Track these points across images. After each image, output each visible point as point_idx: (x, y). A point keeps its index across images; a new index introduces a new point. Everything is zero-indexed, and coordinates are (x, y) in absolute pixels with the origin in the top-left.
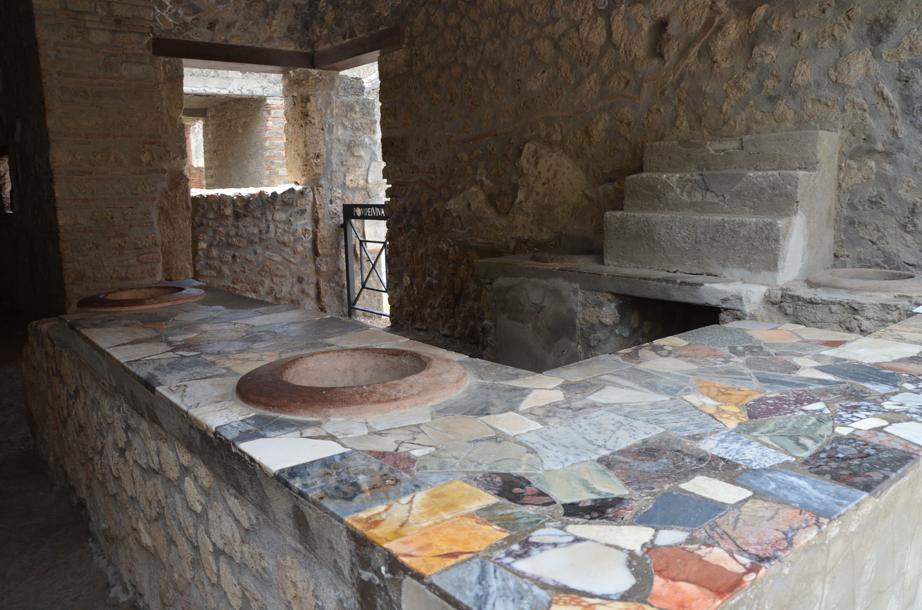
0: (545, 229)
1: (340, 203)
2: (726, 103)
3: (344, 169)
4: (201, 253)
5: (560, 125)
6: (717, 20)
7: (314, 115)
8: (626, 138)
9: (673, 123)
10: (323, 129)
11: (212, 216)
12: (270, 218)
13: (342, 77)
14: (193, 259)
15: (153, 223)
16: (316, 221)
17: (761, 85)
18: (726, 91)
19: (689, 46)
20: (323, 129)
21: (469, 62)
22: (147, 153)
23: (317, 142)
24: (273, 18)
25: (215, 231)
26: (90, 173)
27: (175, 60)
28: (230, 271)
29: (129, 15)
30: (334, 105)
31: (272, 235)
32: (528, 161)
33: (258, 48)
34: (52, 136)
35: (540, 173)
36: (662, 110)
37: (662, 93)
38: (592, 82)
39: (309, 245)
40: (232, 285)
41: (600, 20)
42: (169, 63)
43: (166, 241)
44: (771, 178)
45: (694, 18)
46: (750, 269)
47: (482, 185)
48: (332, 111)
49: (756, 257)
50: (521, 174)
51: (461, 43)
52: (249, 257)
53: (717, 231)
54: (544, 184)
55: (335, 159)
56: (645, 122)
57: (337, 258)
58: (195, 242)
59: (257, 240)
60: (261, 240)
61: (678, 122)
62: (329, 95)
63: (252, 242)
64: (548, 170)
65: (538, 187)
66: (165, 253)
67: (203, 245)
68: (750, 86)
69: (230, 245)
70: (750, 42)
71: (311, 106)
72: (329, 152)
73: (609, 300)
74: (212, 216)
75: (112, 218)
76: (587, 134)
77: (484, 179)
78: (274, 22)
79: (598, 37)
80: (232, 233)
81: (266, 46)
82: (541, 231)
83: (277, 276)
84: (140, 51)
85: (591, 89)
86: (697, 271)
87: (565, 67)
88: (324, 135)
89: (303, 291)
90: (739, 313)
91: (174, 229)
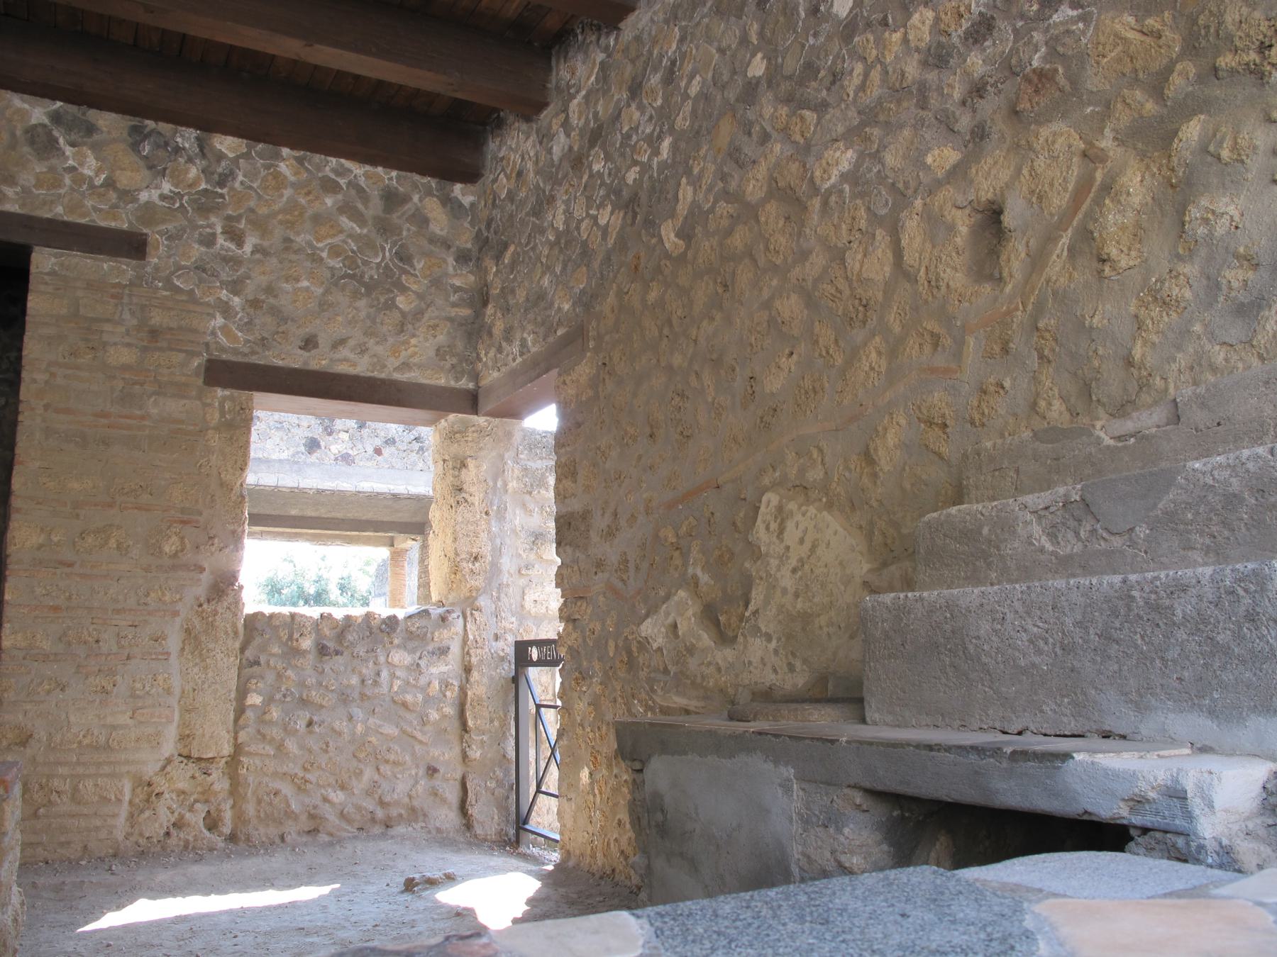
0: (798, 664)
1: (511, 639)
2: (1139, 343)
3: (522, 582)
5: (821, 450)
6: (1099, 175)
7: (472, 489)
8: (940, 456)
9: (1034, 406)
10: (487, 513)
12: (382, 659)
13: (523, 430)
14: (236, 720)
15: (168, 654)
16: (468, 670)
17: (1214, 285)
18: (1136, 316)
19: (1050, 239)
20: (487, 513)
21: (677, 360)
22: (174, 538)
23: (476, 535)
24: (414, 336)
25: (279, 676)
26: (71, 565)
28: (302, 747)
29: (174, 325)
30: (508, 474)
31: (385, 689)
32: (767, 528)
33: (383, 381)
35: (788, 548)
36: (1007, 384)
37: (1005, 350)
38: (874, 355)
39: (450, 710)
40: (301, 774)
41: (880, 233)
42: (232, 398)
43: (188, 688)
44: (1250, 466)
45: (1051, 185)
46: (1212, 713)
47: (697, 584)
48: (505, 484)
49: (1227, 677)
50: (755, 553)
51: (666, 331)
52: (337, 725)
53: (1115, 613)
54: (794, 571)
55: (507, 563)
56: (977, 417)
57: (500, 739)
58: (242, 693)
59: (356, 695)
60: (363, 696)
61: (1042, 404)
62: (501, 457)
64: (802, 541)
65: (787, 581)
67: (255, 699)
68: (1188, 294)
69: (304, 702)
70: (1178, 194)
71: (470, 475)
72: (497, 552)
73: (858, 807)
74: (276, 649)
75: (97, 641)
76: (868, 458)
77: (699, 573)
78: (413, 341)
79: (874, 265)
80: (311, 681)
81: (397, 376)
82: (791, 668)
83: (387, 762)
84: (183, 379)
85: (872, 369)
86: (1072, 726)
87: (826, 335)
88: (488, 523)
89: (435, 793)
90: (1180, 842)
91: (206, 668)
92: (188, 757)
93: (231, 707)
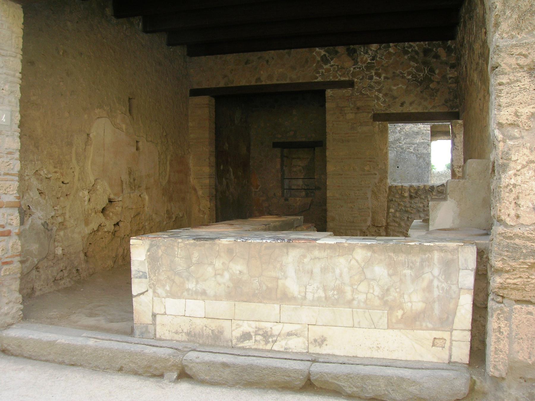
4: (390, 214)
11: (397, 196)
14: (387, 216)
24: (436, 96)
26: (342, 175)
27: (385, 123)
28: (406, 224)
29: (363, 105)
33: (427, 113)
34: (328, 159)
42: (382, 124)
58: (389, 208)
60: (424, 210)
63: (419, 211)
66: (373, 213)
67: (392, 210)
69: (407, 212)
74: (397, 196)
78: (436, 98)
80: (408, 205)
81: (432, 111)
92: (374, 226)
93: (385, 212)
